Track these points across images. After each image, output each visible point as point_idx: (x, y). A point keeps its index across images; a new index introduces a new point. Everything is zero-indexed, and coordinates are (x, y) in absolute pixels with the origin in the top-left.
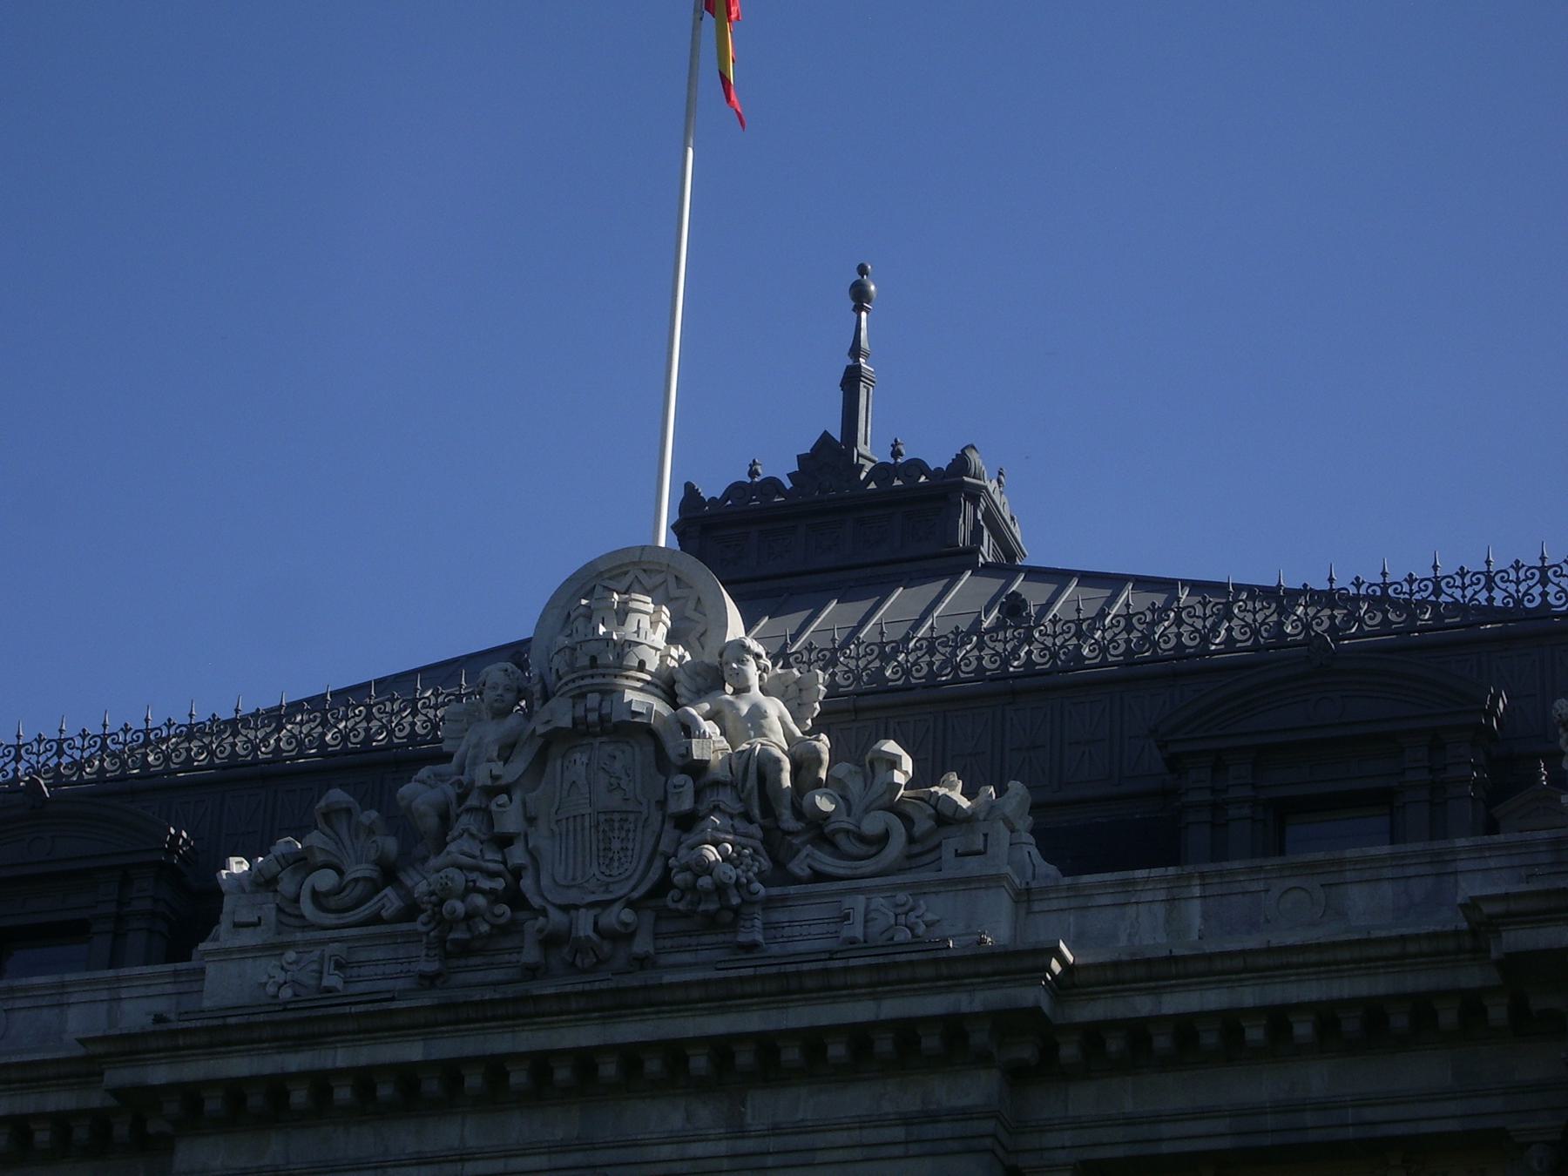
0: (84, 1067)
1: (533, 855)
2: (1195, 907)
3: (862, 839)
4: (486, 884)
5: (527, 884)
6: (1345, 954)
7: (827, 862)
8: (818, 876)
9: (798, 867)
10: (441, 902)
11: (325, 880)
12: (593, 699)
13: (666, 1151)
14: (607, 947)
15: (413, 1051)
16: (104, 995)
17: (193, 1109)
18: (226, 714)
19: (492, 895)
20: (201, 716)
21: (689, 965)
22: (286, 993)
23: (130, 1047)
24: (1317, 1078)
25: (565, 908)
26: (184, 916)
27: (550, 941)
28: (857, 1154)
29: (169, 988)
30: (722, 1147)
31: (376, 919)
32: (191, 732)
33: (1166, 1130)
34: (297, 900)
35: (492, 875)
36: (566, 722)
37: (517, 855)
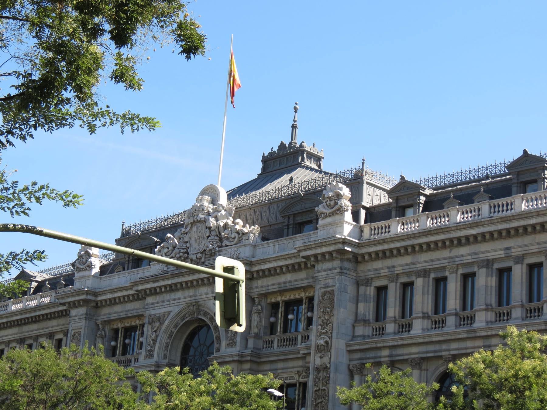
1: (191, 245)
2: (277, 247)
4: (182, 251)
5: (189, 250)
6: (286, 257)
7: (228, 243)
8: (227, 246)
9: (224, 244)
13: (204, 296)
14: (198, 260)
19: (184, 253)
24: (289, 277)
33: (269, 288)
35: (184, 249)
36: (192, 221)
37: (188, 245)
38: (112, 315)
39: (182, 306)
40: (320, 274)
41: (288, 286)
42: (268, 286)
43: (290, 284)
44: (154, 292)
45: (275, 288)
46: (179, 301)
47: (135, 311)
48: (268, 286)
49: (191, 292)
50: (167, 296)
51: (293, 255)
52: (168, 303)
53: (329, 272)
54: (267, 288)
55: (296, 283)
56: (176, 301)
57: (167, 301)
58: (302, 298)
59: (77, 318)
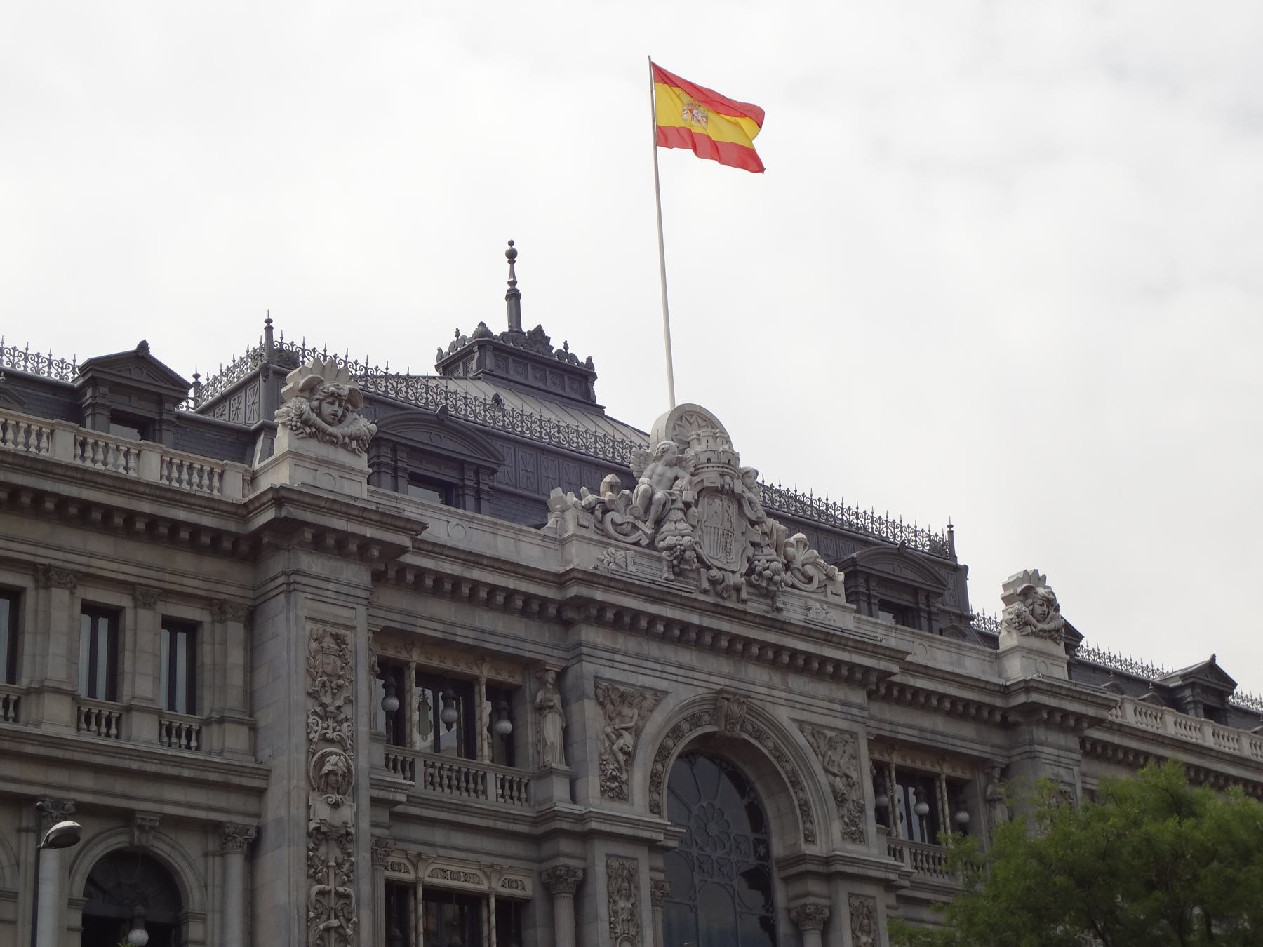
0: (561, 580)
3: (803, 574)
10: (684, 551)
11: (618, 518)
12: (727, 479)
15: (695, 619)
16: (512, 536)
17: (599, 615)
18: (403, 373)
20: (392, 372)
21: (755, 607)
22: (612, 566)
23: (590, 578)
25: (720, 569)
26: (533, 508)
27: (713, 582)
28: (825, 711)
29: (540, 543)
30: (783, 695)
31: (637, 544)
32: (387, 377)
34: (601, 522)
38: (421, 622)
39: (700, 691)
40: (1046, 749)
41: (941, 743)
42: (898, 725)
43: (946, 740)
44: (623, 622)
45: (910, 735)
46: (691, 674)
47: (511, 643)
48: (898, 725)
49: (725, 666)
50: (653, 649)
51: (983, 685)
52: (658, 667)
53: (1062, 753)
54: (894, 728)
55: (958, 742)
56: (681, 672)
57: (654, 660)
58: (407, 664)
59: (331, 586)
